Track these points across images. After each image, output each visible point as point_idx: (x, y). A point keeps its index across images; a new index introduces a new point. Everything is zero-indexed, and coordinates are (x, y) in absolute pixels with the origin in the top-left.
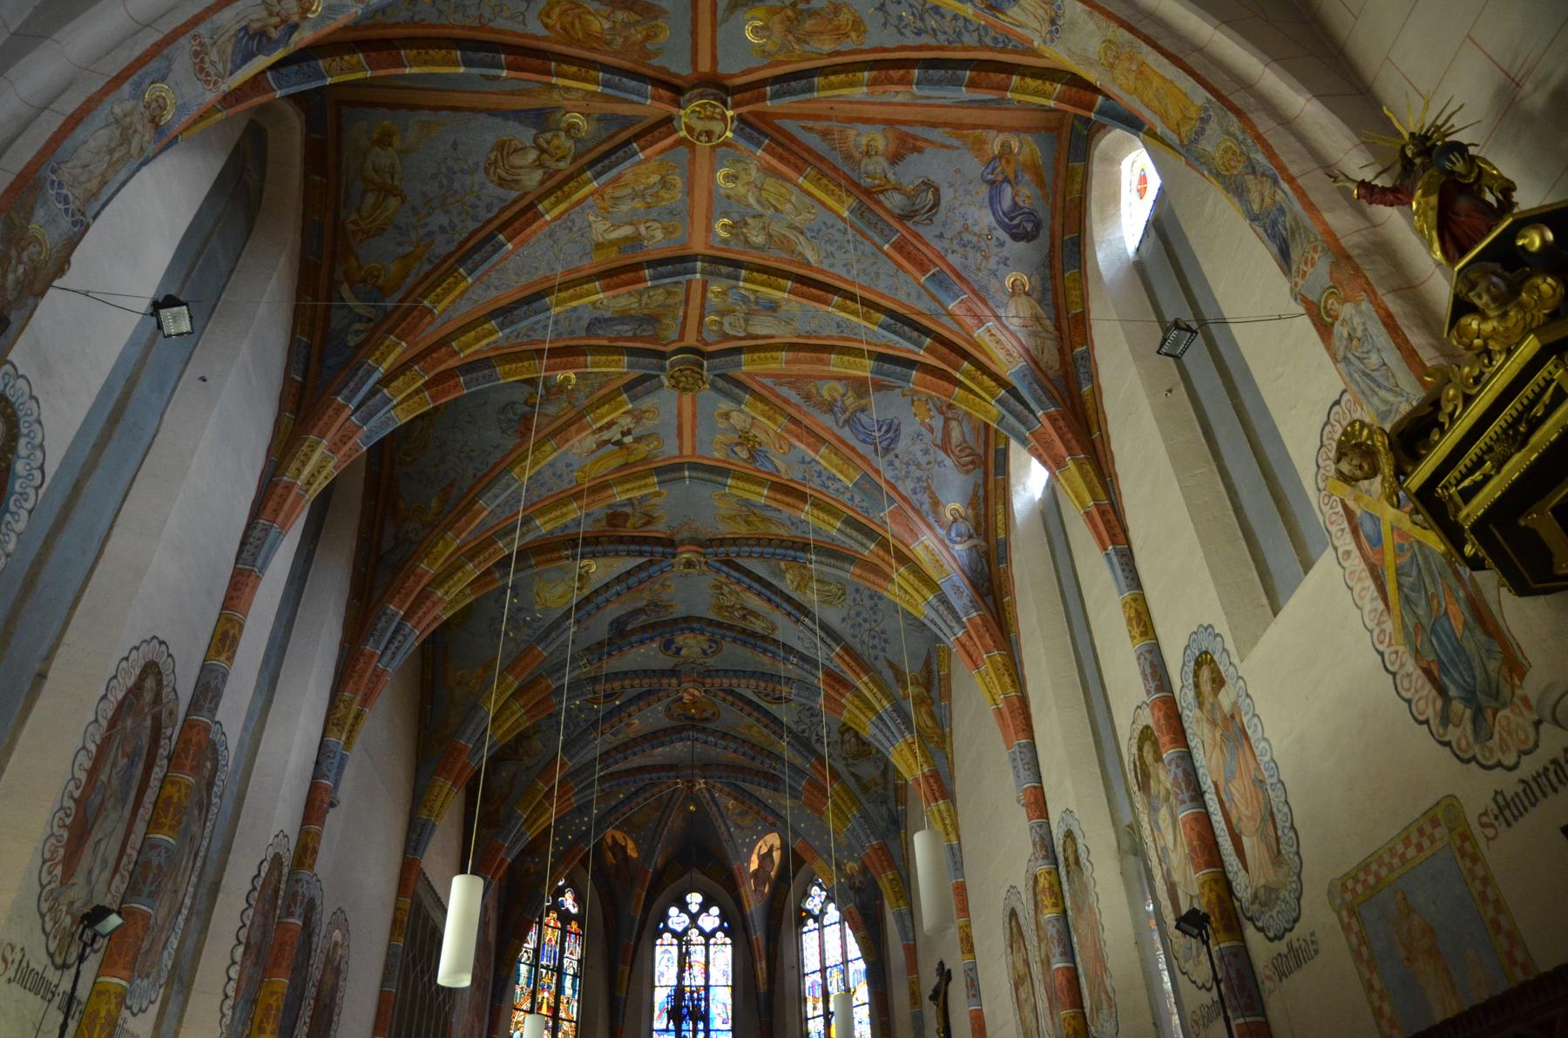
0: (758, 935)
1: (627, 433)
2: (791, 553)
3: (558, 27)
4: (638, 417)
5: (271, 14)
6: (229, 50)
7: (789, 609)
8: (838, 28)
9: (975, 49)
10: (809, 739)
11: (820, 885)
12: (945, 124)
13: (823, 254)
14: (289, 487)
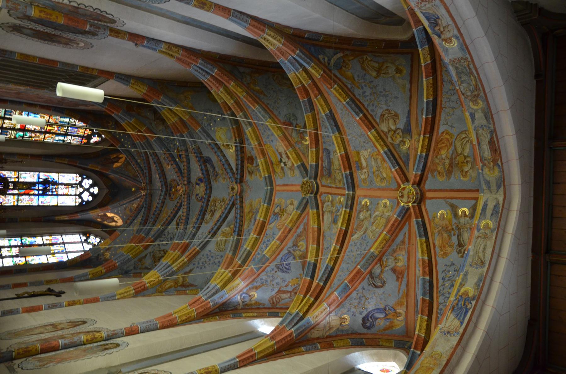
0: (79, 216)
1: (285, 165)
2: (237, 229)
3: (442, 137)
4: (291, 168)
5: (444, 27)
6: (431, 12)
7: (215, 229)
8: (444, 247)
9: (437, 301)
10: (161, 237)
11: (100, 242)
12: (408, 290)
13: (356, 241)
14: (263, 31)
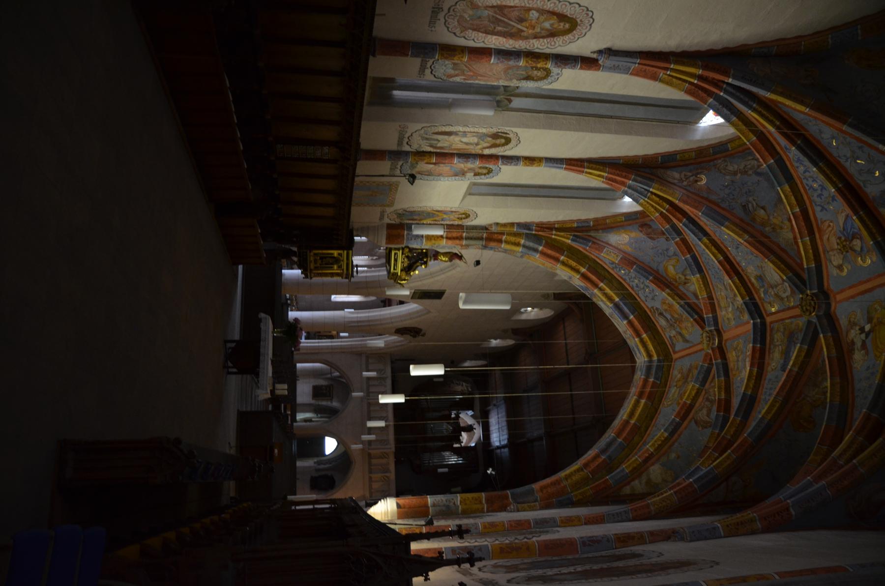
1: (862, 330)
